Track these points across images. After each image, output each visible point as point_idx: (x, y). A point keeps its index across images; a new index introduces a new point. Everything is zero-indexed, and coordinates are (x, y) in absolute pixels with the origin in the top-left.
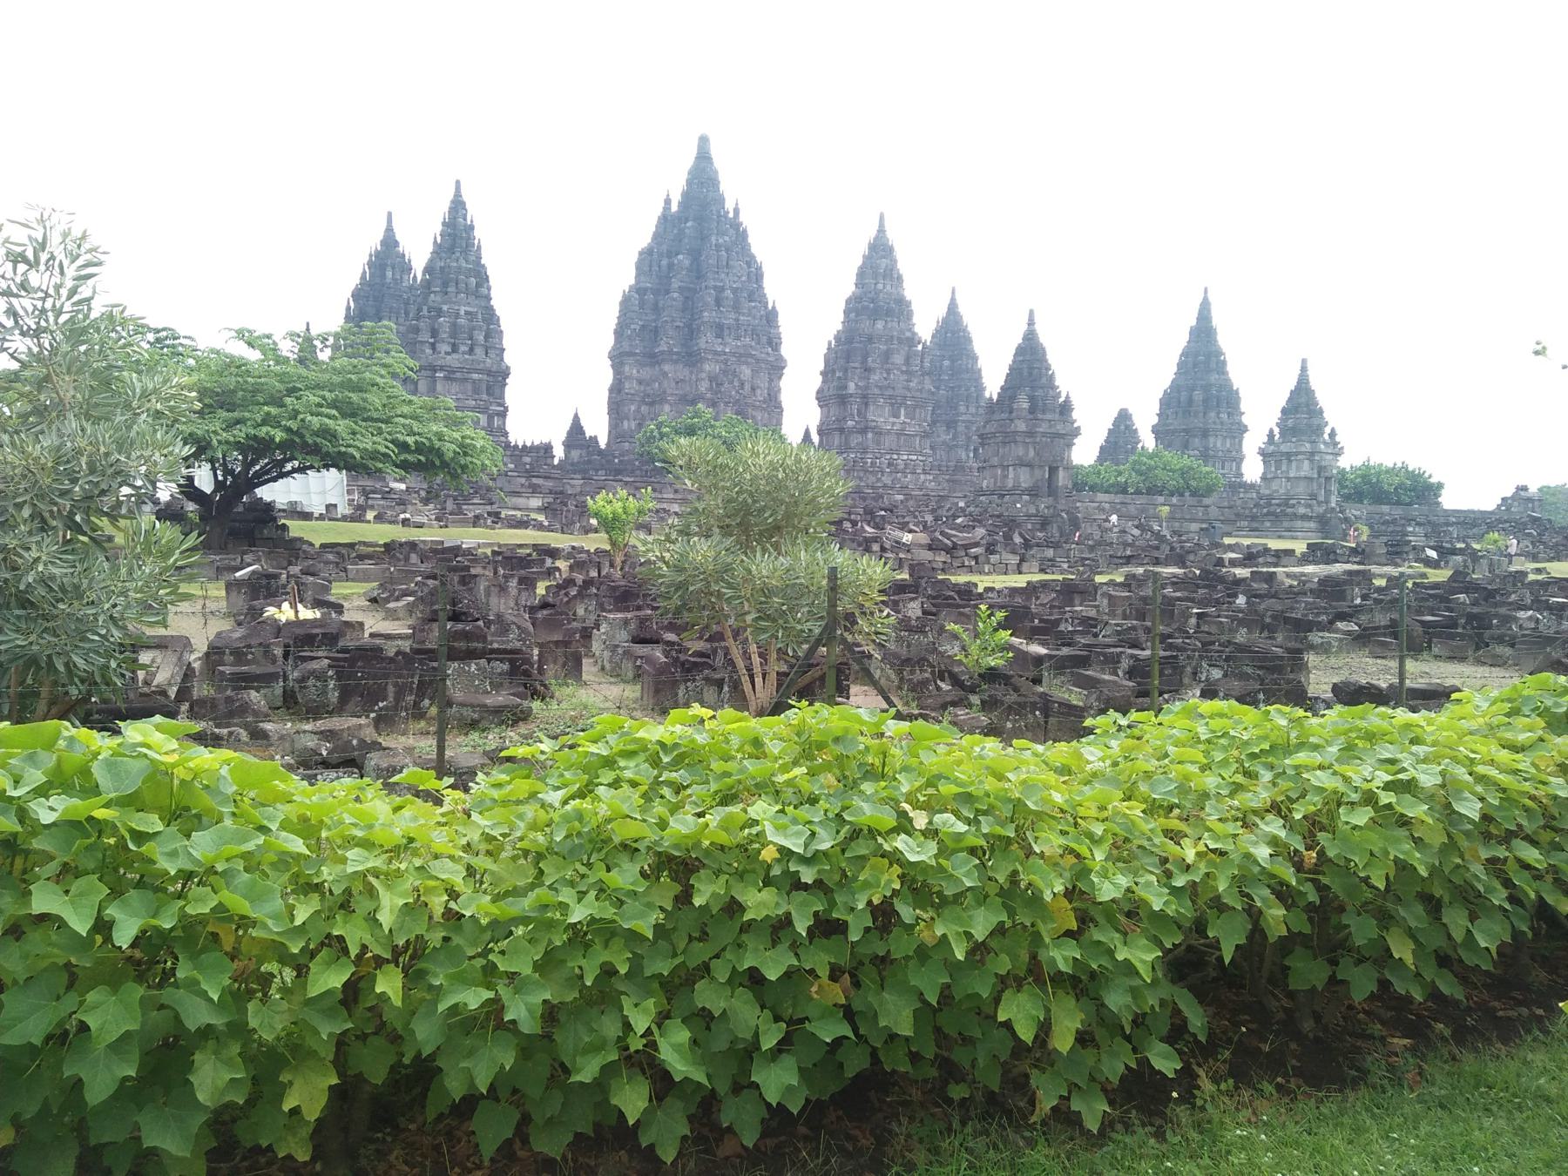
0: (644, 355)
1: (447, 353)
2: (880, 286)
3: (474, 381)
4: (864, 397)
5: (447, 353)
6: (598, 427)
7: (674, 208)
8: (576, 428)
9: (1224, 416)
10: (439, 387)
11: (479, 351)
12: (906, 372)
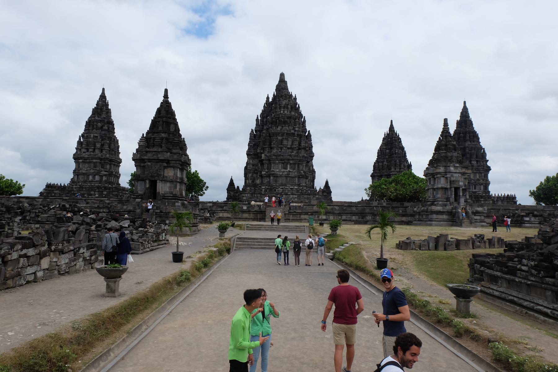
0: (255, 155)
1: (84, 152)
2: (282, 112)
3: (94, 163)
4: (269, 160)
5: (84, 152)
6: (240, 183)
7: (270, 100)
8: (232, 183)
9: (474, 163)
10: (81, 166)
11: (97, 151)
12: (291, 148)
